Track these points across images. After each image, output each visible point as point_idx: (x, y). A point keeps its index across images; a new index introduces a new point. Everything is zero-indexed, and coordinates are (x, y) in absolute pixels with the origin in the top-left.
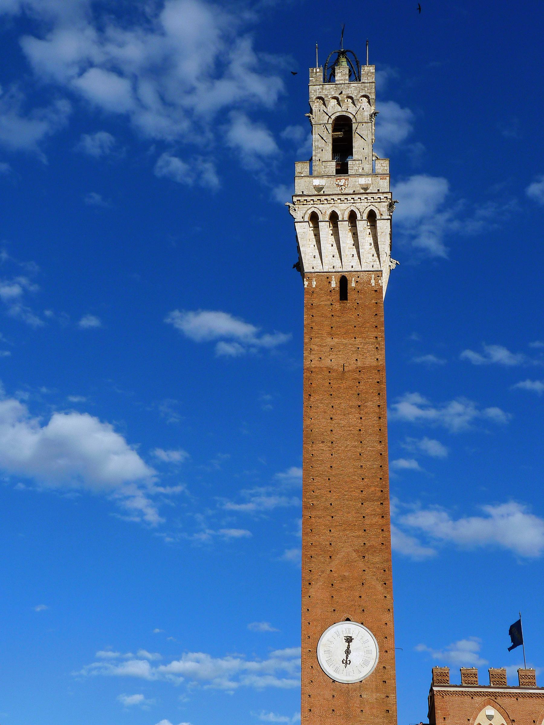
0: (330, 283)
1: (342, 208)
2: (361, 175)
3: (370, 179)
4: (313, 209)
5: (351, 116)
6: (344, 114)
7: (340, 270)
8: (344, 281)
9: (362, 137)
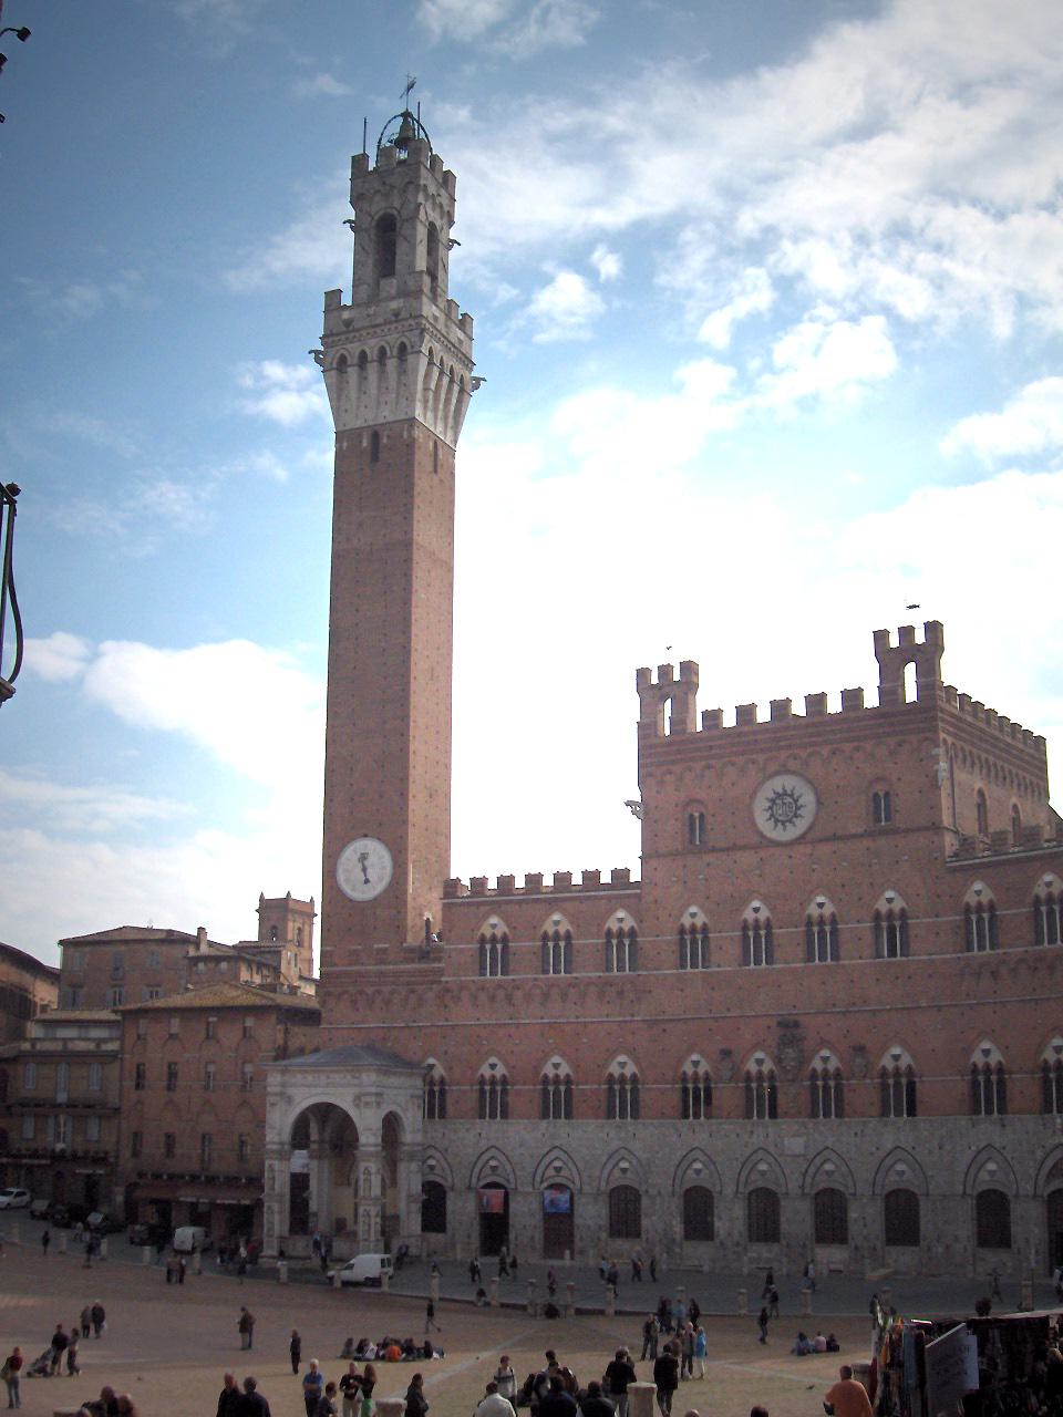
0: (361, 442)
1: (372, 345)
2: (393, 298)
3: (402, 300)
4: (342, 351)
5: (395, 213)
6: (389, 211)
7: (371, 423)
8: (376, 436)
9: (405, 238)
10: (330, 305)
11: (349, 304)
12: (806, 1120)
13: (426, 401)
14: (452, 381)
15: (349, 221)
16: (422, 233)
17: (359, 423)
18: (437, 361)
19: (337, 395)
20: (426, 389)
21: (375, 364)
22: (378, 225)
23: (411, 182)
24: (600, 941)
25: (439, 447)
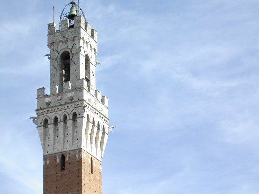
2: (70, 91)
5: (69, 51)
7: (61, 151)
8: (63, 157)
10: (40, 95)
11: (49, 95)
13: (86, 140)
14: (99, 129)
15: (47, 55)
16: (82, 60)
17: (55, 151)
18: (91, 120)
19: (45, 137)
20: (86, 134)
21: (62, 123)
22: (61, 55)
23: (76, 36)
25: (94, 161)
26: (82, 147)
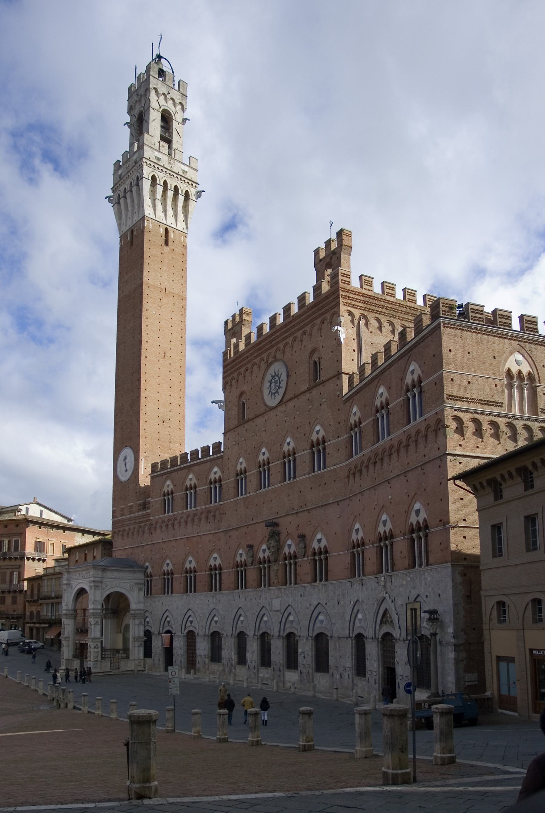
8: (132, 232)
12: (281, 587)
15: (127, 123)
24: (207, 487)
26: (145, 215)
